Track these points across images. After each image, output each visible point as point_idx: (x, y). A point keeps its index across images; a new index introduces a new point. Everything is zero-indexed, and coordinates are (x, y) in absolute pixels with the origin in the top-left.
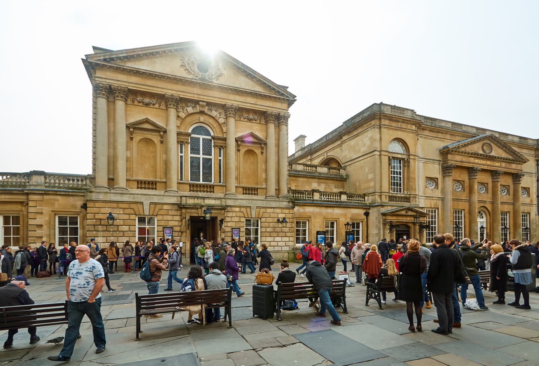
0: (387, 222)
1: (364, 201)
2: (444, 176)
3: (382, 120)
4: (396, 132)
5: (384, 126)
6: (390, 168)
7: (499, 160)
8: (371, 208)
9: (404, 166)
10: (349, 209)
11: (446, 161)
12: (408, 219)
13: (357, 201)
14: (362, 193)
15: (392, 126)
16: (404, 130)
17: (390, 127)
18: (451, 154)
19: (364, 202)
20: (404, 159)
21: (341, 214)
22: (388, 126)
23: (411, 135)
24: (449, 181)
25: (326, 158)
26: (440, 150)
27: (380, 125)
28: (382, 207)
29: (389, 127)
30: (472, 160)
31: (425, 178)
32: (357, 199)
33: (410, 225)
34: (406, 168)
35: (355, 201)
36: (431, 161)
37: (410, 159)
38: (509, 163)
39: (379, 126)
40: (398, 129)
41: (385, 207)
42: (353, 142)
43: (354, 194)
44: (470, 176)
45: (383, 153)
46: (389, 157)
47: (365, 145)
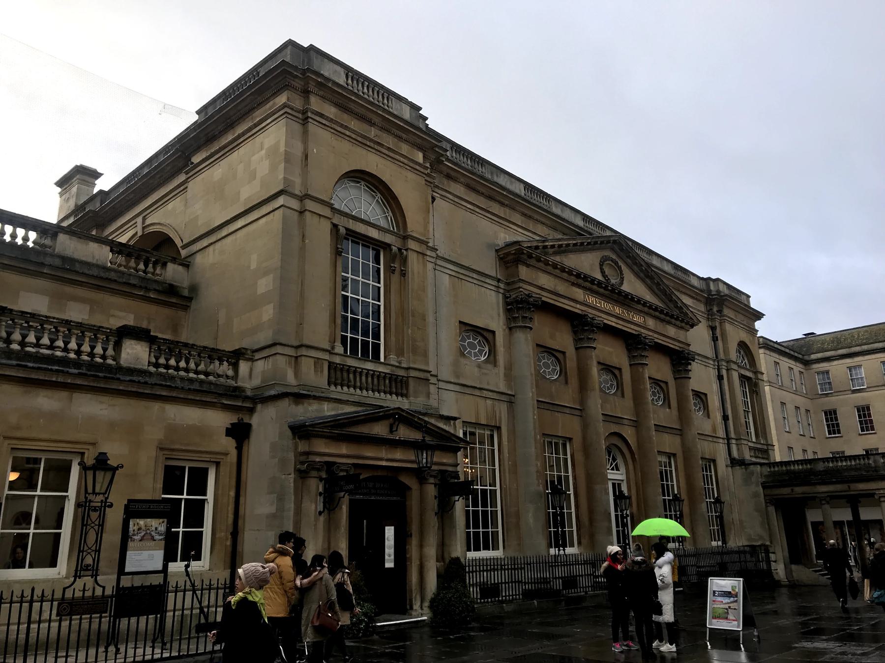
0: (313, 466)
1: (235, 377)
2: (510, 329)
3: (313, 99)
4: (360, 151)
5: (318, 118)
6: (339, 268)
7: (640, 307)
8: (259, 406)
9: (390, 270)
10: (156, 406)
11: (514, 282)
12: (398, 454)
13: (202, 377)
14: (228, 346)
15: (346, 128)
16: (387, 152)
17: (339, 129)
18: (528, 266)
19: (232, 383)
20: (389, 245)
21: (112, 425)
22: (331, 120)
23: (411, 175)
24: (524, 343)
25: (140, 234)
26: (497, 251)
27: (304, 112)
28: (297, 403)
29: (339, 130)
30: (579, 294)
31: (457, 324)
32: (202, 367)
33: (406, 480)
34: (395, 278)
35: (191, 375)
36: (475, 276)
37: (406, 250)
38: (662, 320)
39: (300, 116)
40: (368, 143)
41: (310, 404)
42: (217, 172)
43: (186, 345)
44: (577, 340)
45: (310, 205)
46: (335, 226)
47: (253, 176)
